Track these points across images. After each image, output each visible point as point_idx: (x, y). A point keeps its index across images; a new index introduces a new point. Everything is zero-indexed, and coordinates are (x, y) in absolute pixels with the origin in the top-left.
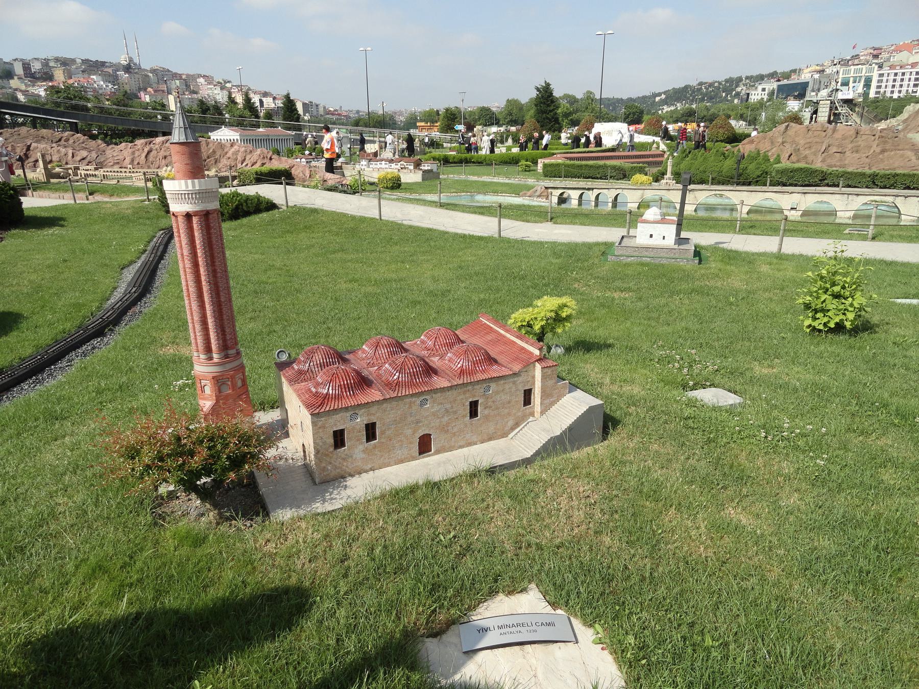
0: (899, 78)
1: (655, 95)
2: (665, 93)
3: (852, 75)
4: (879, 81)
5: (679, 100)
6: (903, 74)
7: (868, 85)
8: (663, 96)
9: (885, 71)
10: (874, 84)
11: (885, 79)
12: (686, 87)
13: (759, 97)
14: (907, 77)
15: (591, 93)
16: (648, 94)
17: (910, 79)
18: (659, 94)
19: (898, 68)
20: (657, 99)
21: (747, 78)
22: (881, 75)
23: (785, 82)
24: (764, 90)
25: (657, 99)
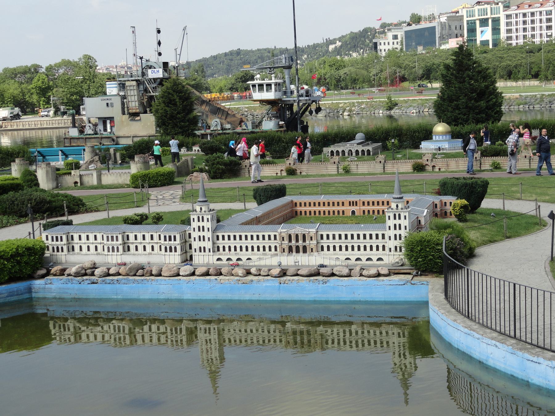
0: (529, 19)
1: (331, 42)
2: (340, 39)
3: (477, 17)
4: (508, 24)
5: (355, 48)
6: (533, 14)
7: (496, 30)
8: (339, 44)
9: (512, 11)
10: (503, 28)
11: (513, 20)
12: (366, 31)
13: (390, 47)
14: (537, 17)
15: (90, 58)
16: (320, 41)
17: (541, 20)
18: (333, 42)
19: (527, 6)
20: (331, 47)
22: (508, 16)
24: (395, 37)
25: (331, 47)
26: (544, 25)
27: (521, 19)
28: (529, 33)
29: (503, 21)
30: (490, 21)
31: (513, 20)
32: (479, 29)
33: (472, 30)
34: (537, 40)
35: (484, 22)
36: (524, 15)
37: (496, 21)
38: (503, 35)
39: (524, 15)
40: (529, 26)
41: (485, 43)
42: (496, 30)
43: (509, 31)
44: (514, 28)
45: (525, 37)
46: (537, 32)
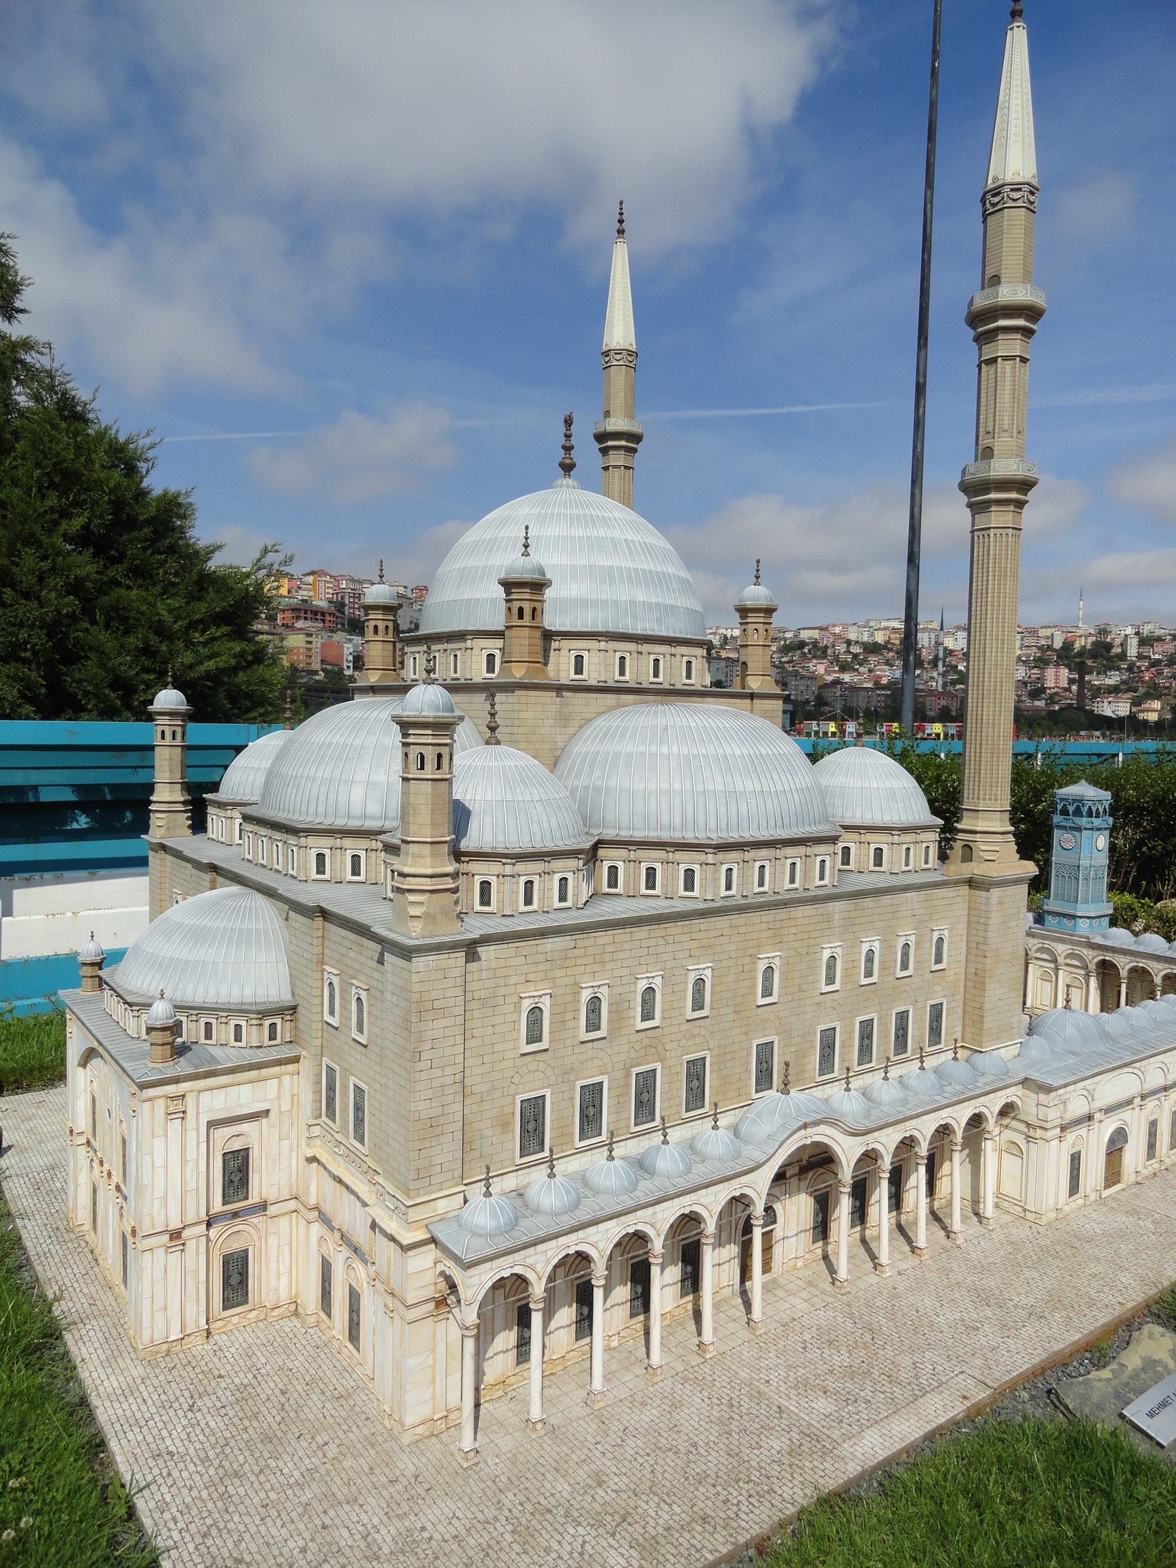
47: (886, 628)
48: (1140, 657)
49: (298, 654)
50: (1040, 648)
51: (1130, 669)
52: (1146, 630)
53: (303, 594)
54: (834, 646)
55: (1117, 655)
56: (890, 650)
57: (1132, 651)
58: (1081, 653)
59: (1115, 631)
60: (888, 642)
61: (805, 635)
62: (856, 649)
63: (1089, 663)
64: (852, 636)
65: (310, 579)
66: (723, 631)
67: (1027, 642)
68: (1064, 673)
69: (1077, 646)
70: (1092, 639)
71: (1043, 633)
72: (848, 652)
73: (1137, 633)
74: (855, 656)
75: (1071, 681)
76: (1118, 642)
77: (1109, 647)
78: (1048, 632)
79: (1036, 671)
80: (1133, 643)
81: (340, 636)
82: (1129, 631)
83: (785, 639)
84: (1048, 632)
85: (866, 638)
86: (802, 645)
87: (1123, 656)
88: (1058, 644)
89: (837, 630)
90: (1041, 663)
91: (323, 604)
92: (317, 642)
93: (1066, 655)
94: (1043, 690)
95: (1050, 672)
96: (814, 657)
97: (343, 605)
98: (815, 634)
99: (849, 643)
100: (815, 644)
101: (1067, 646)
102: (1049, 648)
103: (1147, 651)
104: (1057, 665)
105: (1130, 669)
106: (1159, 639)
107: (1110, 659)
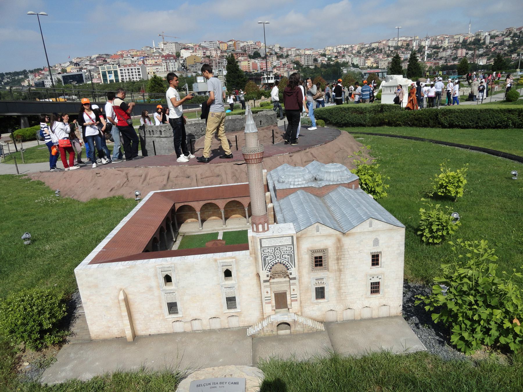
4: (121, 73)
7: (116, 75)
10: (119, 75)
14: (134, 71)
21: (7, 74)
22: (121, 70)
23: (65, 74)
26: (137, 74)
27: (127, 71)
28: (131, 77)
29: (119, 72)
30: (113, 72)
31: (124, 72)
32: (108, 75)
33: (104, 75)
34: (135, 79)
35: (110, 72)
36: (132, 69)
37: (116, 72)
38: (120, 78)
39: (128, 70)
40: (131, 74)
41: (111, 81)
42: (116, 75)
43: (122, 76)
44: (124, 75)
45: (129, 78)
46: (135, 77)
47: (401, 40)
48: (490, 43)
49: (246, 67)
50: (455, 43)
51: (487, 48)
52: (492, 33)
53: (232, 48)
54: (384, 48)
55: (482, 43)
56: (403, 48)
57: (488, 41)
58: (470, 44)
59: (482, 34)
60: (402, 45)
61: (374, 45)
62: (392, 49)
63: (473, 47)
64: (390, 44)
65: (230, 43)
66: (343, 46)
67: (450, 41)
68: (464, 51)
69: (468, 41)
70: (474, 38)
71: (456, 37)
72: (389, 50)
73: (489, 35)
74: (392, 51)
75: (467, 54)
76: (483, 38)
77: (479, 40)
78: (458, 37)
79: (454, 51)
80: (488, 38)
81: (253, 61)
82: (487, 34)
83: (367, 47)
84: (458, 37)
85: (394, 45)
86: (373, 49)
87: (484, 43)
88: (461, 41)
89: (384, 42)
90: (456, 48)
91: (240, 51)
92: (251, 63)
93: (465, 45)
94: (457, 58)
95: (459, 51)
96: (378, 53)
97: (245, 51)
98: (377, 45)
99: (389, 47)
100: (378, 48)
101: (465, 41)
102: (458, 42)
103: (493, 41)
104: (462, 48)
105: (487, 48)
106: (497, 36)
107: (480, 45)
